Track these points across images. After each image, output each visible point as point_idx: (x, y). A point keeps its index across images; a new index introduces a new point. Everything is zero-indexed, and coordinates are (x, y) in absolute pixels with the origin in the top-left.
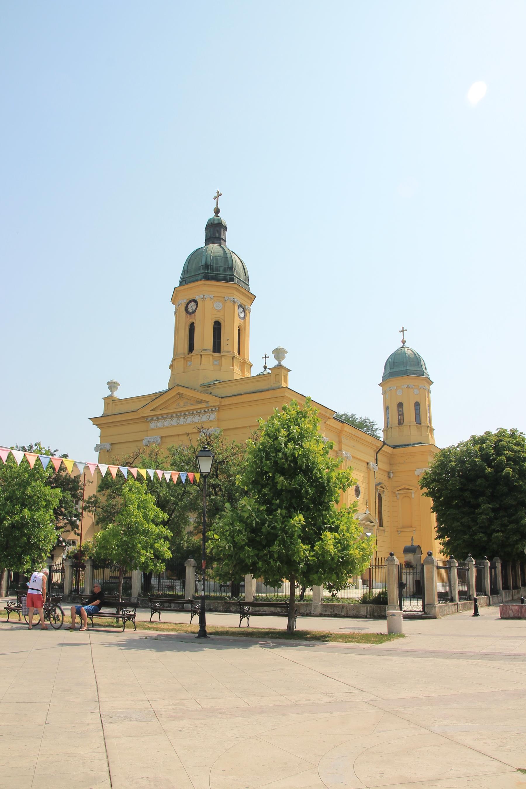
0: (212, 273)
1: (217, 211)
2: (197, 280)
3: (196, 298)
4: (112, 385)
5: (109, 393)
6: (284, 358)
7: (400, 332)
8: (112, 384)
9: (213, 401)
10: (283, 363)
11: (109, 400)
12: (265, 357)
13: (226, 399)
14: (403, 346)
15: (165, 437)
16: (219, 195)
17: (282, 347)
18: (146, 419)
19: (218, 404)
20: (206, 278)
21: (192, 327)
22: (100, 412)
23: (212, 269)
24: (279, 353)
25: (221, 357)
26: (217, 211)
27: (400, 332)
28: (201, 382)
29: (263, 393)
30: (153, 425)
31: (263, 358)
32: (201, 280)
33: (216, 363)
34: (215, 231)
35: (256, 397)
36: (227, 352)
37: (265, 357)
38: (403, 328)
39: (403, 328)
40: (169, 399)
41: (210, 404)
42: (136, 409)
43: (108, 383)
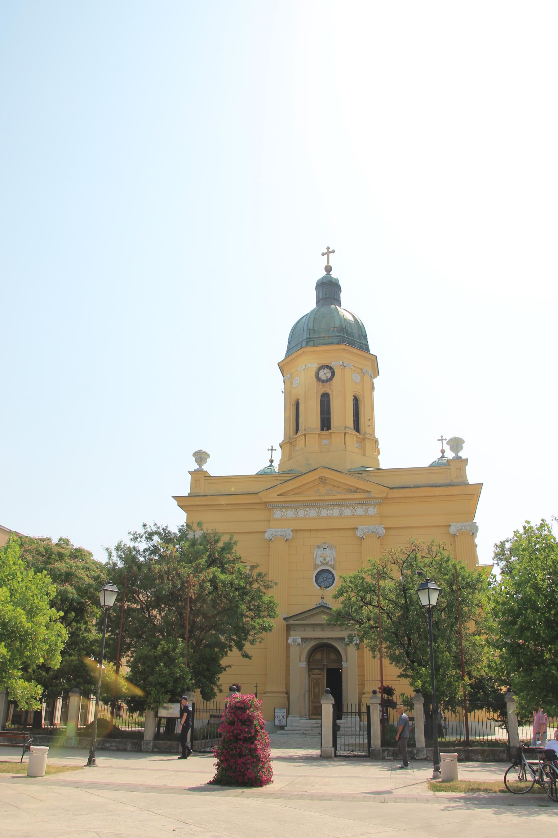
0: (348, 339)
1: (328, 269)
2: (331, 344)
3: (333, 364)
4: (201, 457)
5: (195, 466)
6: (462, 448)
7: (439, 440)
8: (203, 456)
9: (376, 492)
10: (463, 454)
11: (198, 476)
12: (272, 450)
13: (395, 490)
14: (443, 456)
15: (297, 530)
16: (328, 252)
17: (458, 436)
18: (267, 506)
19: (385, 495)
20: (341, 341)
22: (186, 491)
23: (348, 334)
25: (364, 439)
26: (328, 269)
27: (439, 440)
28: (349, 466)
29: (450, 488)
30: (278, 514)
31: (269, 450)
32: (339, 343)
33: (357, 445)
34: (329, 290)
35: (437, 491)
36: (370, 434)
37: (272, 450)
38: (442, 437)
39: (442, 437)
40: (304, 485)
41: (373, 495)
42: (257, 491)
43: (194, 454)
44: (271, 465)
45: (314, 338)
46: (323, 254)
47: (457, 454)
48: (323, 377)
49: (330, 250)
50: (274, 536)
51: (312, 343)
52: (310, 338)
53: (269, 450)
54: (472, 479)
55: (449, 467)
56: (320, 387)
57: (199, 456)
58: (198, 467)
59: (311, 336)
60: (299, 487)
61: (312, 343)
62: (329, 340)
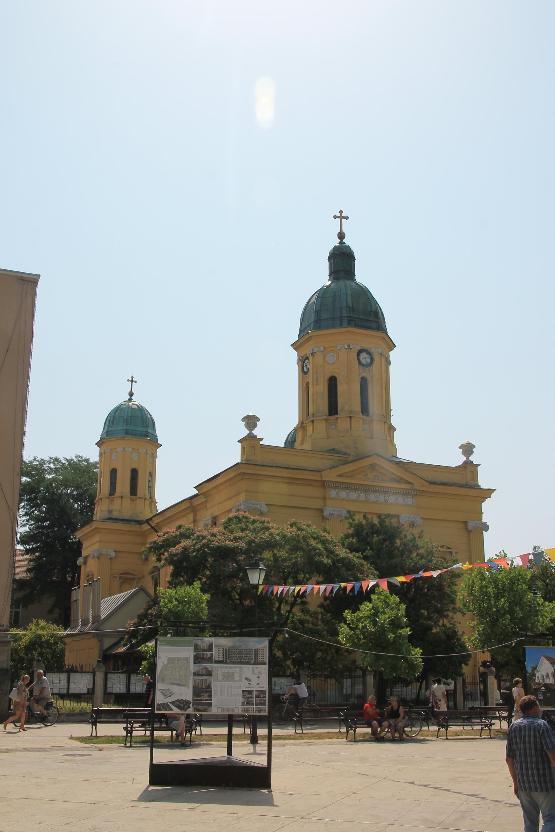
1: (341, 236)
4: (251, 421)
18: (323, 484)
19: (424, 489)
21: (364, 383)
24: (468, 449)
26: (341, 236)
30: (333, 493)
31: (128, 380)
34: (342, 261)
41: (415, 487)
44: (130, 400)
45: (355, 318)
46: (335, 217)
47: (468, 458)
48: (364, 362)
49: (343, 215)
50: (331, 515)
51: (353, 323)
52: (350, 317)
53: (128, 380)
54: (483, 482)
55: (465, 470)
56: (361, 371)
57: (252, 421)
58: (248, 432)
59: (351, 315)
60: (353, 471)
61: (353, 323)
62: (344, 315)
